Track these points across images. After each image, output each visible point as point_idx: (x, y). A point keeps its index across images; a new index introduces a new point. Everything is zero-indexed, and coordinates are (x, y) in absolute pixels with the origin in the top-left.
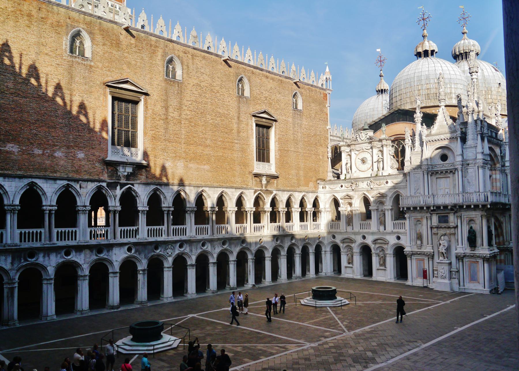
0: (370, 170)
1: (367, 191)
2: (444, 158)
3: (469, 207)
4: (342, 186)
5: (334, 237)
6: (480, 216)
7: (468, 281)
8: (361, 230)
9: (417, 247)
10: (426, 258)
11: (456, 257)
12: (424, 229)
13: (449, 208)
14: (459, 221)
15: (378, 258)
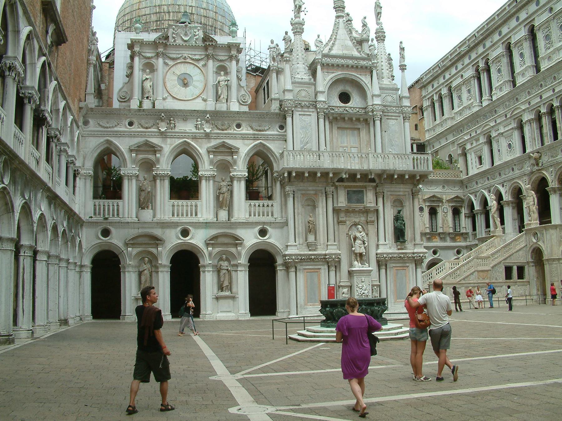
0: (199, 100)
1: (194, 138)
2: (345, 98)
3: (401, 176)
4: (131, 124)
5: (106, 233)
6: (411, 193)
7: (393, 302)
8: (175, 219)
9: (309, 246)
10: (326, 267)
11: (378, 262)
12: (323, 215)
13: (373, 177)
14: (380, 200)
15: (215, 274)
